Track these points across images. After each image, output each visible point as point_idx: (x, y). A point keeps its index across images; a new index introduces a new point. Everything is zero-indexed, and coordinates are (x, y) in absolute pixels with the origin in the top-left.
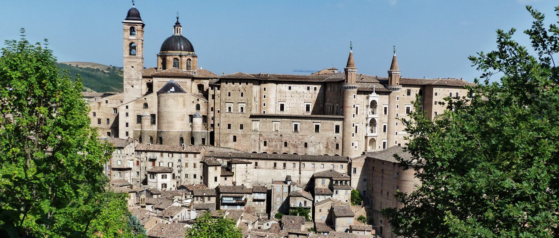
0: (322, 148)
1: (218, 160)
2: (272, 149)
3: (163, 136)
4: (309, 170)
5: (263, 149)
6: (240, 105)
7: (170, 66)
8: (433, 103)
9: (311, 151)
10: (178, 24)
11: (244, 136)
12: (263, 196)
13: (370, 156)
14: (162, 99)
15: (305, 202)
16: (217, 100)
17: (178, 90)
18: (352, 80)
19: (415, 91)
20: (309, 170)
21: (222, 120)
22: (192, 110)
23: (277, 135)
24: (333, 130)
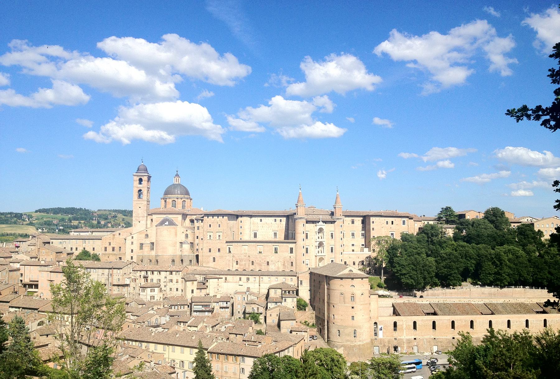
0: (280, 266)
1: (196, 276)
2: (242, 267)
3: (158, 258)
4: (267, 282)
5: (236, 267)
6: (218, 234)
7: (169, 206)
8: (371, 229)
9: (272, 268)
10: (177, 175)
11: (221, 257)
12: (229, 304)
13: (313, 271)
15: (258, 308)
17: (171, 223)
18: (301, 213)
19: (358, 221)
20: (267, 282)
22: (183, 238)
24: (288, 251)
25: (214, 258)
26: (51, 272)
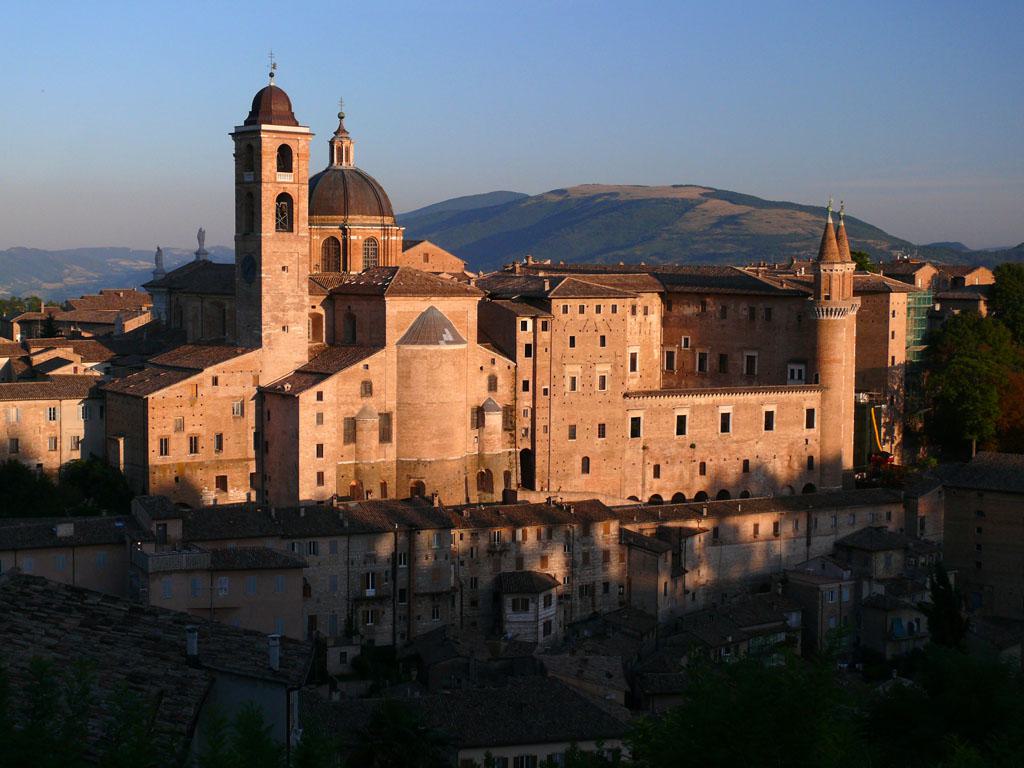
11: (609, 456)
14: (420, 369)
16: (543, 360)
21: (555, 417)
23: (682, 446)
25: (586, 462)
26: (208, 570)
